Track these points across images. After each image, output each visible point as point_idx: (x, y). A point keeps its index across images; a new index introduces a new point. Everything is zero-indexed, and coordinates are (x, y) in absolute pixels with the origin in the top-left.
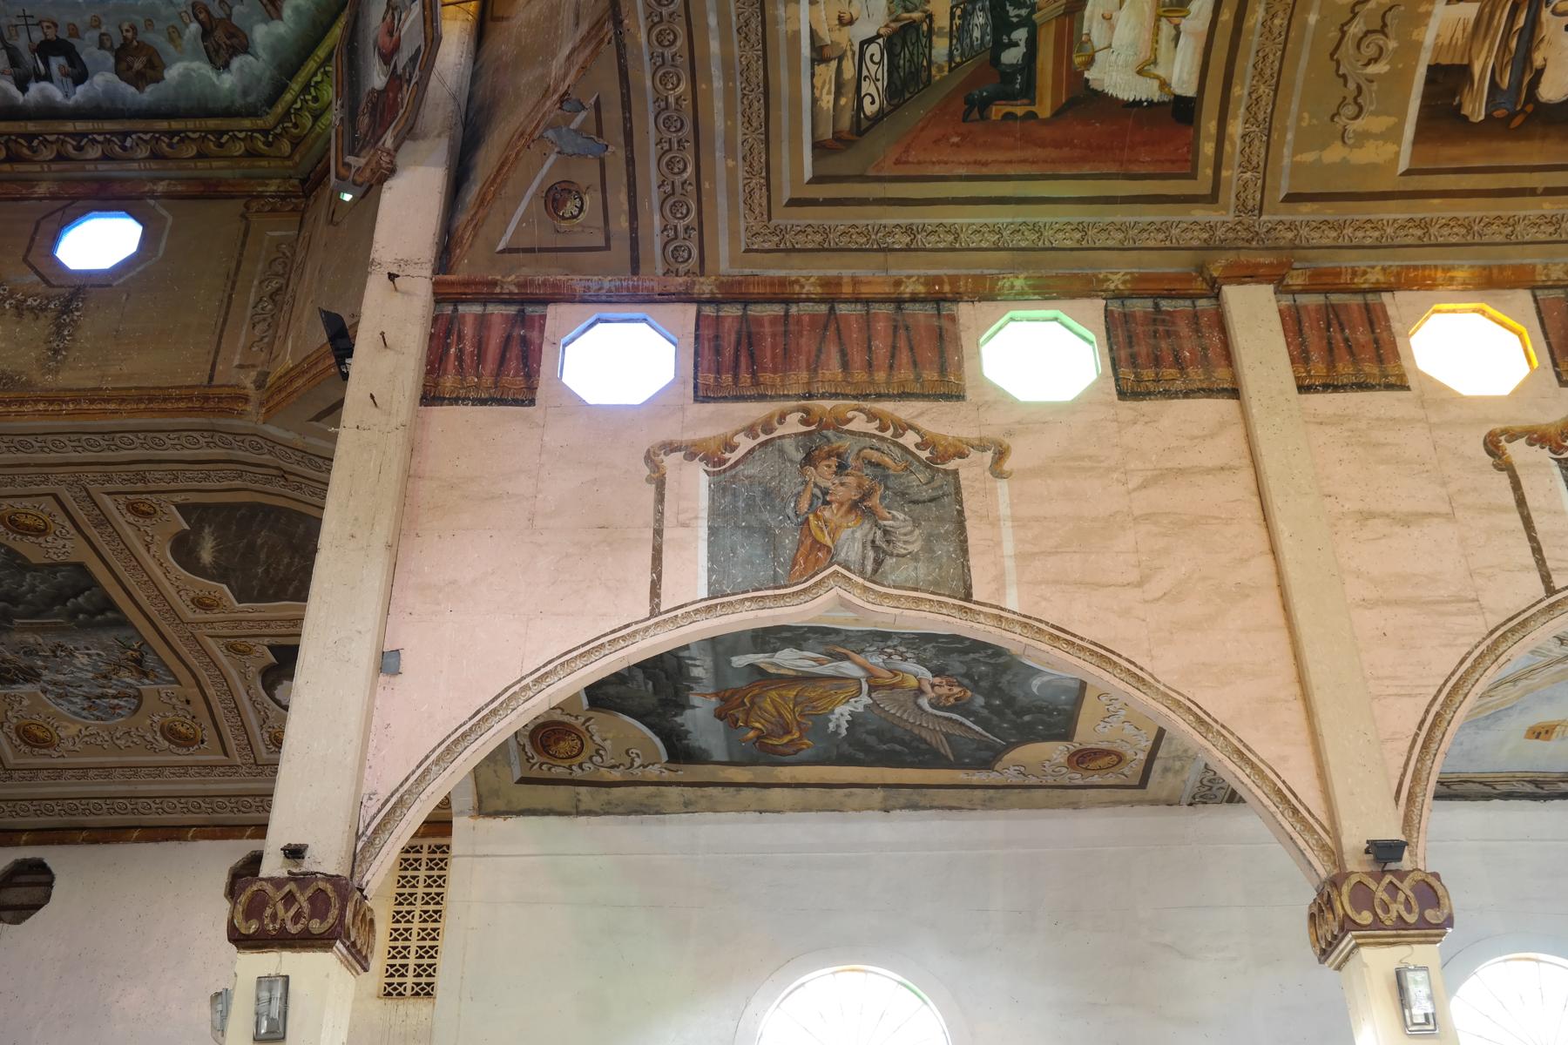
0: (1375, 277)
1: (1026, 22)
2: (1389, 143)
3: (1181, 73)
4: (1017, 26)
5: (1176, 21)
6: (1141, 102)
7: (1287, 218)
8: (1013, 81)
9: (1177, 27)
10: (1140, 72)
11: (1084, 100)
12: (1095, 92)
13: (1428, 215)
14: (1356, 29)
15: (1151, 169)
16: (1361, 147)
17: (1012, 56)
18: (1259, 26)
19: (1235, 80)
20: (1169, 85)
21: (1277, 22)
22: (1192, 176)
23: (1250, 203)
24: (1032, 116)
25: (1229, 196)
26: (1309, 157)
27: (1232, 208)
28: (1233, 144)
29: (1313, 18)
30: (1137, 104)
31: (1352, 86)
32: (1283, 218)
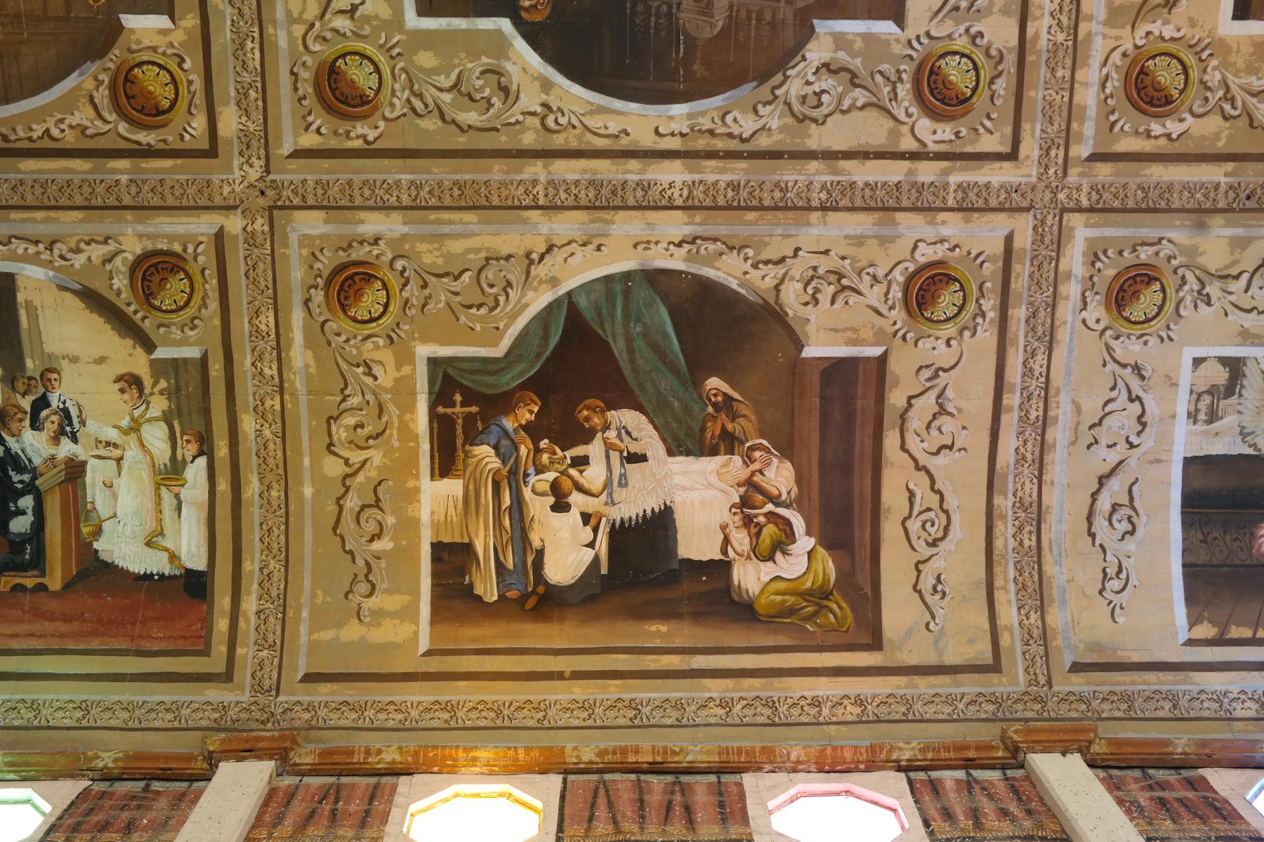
0: (390, 756)
1: (30, 488)
2: (405, 621)
3: (189, 545)
4: (22, 493)
5: (176, 489)
6: (152, 575)
7: (305, 699)
8: (23, 552)
9: (177, 496)
10: (148, 544)
11: (95, 573)
12: (105, 564)
13: (455, 698)
14: (352, 503)
15: (163, 646)
16: (379, 625)
17: (20, 525)
18: (257, 497)
19: (245, 554)
20: (179, 558)
21: (274, 493)
22: (206, 653)
23: (267, 683)
24: (42, 588)
25: (244, 675)
26: (326, 635)
27: (248, 689)
28: (247, 621)
29: (308, 491)
30: (148, 577)
31: (360, 562)
32: (300, 698)
